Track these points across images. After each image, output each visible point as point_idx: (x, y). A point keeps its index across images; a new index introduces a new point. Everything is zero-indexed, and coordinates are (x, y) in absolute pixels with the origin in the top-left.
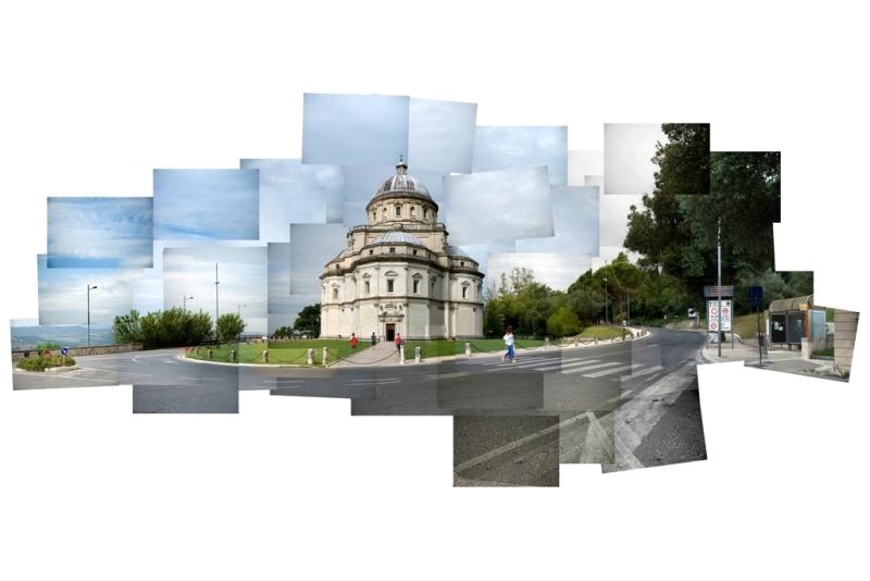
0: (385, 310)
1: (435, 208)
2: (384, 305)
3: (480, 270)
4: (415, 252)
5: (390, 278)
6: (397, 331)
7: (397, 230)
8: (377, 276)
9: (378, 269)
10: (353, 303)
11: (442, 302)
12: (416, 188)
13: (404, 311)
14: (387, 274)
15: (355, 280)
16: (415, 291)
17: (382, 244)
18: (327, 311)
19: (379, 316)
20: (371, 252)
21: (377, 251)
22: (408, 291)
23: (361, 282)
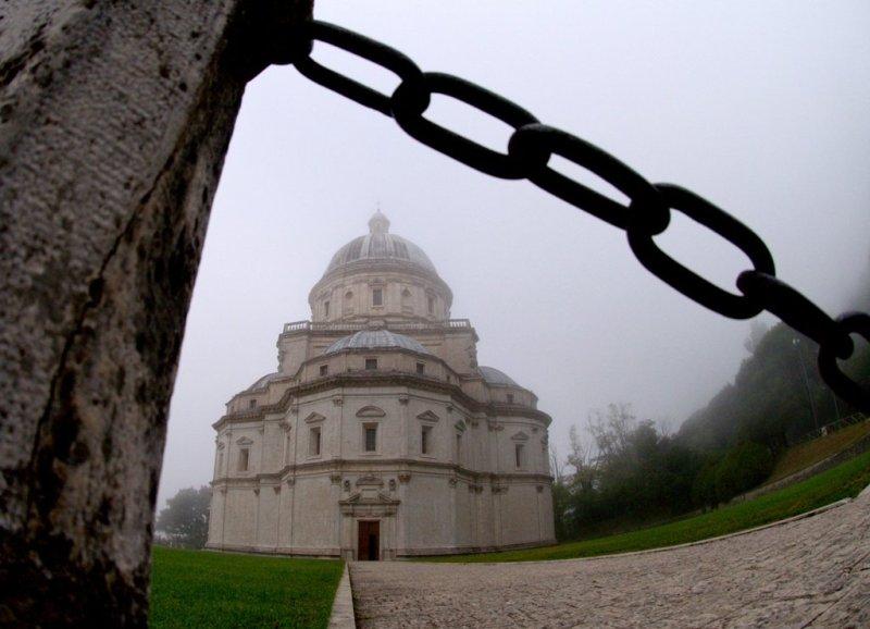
0: (355, 490)
2: (353, 480)
3: (541, 407)
4: (420, 367)
5: (370, 421)
6: (385, 542)
7: (372, 329)
8: (339, 420)
10: (278, 477)
11: (475, 476)
12: (411, 257)
13: (401, 492)
14: (359, 414)
15: (286, 427)
16: (424, 451)
17: (348, 351)
18: (224, 492)
19: (342, 504)
20: (323, 369)
21: (336, 367)
22: (410, 448)
23: (302, 432)
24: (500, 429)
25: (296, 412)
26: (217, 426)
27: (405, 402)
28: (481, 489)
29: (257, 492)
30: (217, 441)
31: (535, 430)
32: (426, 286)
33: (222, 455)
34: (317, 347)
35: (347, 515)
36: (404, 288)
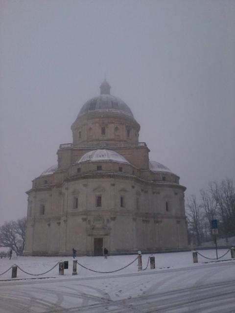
1: (137, 127)
5: (98, 194)
8: (85, 192)
9: (85, 185)
14: (94, 190)
16: (122, 206)
20: (79, 170)
24: (159, 193)
25: (67, 189)
26: (28, 193)
27: (113, 185)
28: (149, 221)
29: (49, 225)
30: (28, 200)
31: (176, 194)
32: (127, 125)
33: (31, 208)
34: (77, 155)
35: (89, 235)
36: (116, 126)
